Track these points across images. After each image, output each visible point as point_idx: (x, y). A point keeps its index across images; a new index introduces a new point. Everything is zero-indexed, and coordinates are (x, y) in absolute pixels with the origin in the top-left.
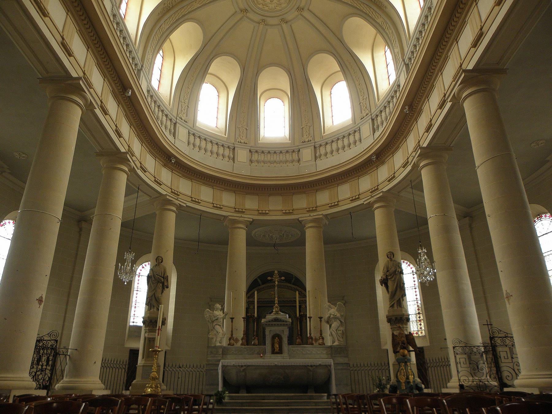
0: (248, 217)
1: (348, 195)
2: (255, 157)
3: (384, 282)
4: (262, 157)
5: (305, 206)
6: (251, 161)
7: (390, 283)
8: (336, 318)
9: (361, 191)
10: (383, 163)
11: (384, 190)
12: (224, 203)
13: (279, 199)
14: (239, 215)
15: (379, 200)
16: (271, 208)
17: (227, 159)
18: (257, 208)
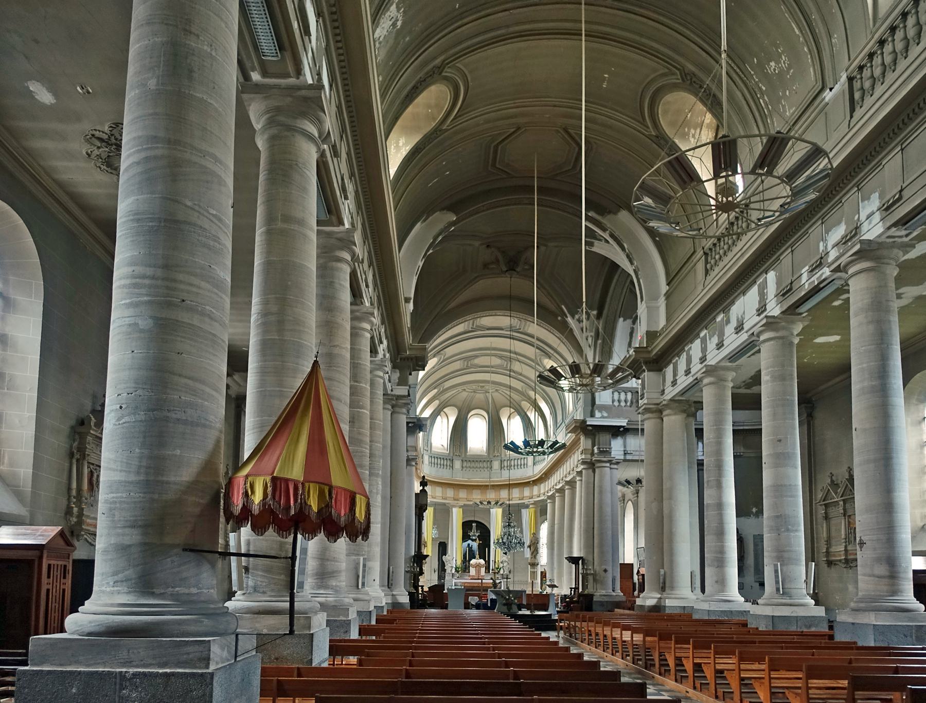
0: (461, 503)
1: (518, 496)
2: (465, 464)
3: (529, 547)
4: (469, 464)
5: (494, 497)
6: (462, 467)
7: (532, 548)
8: (505, 561)
9: (525, 495)
10: (536, 485)
11: (535, 500)
12: (448, 495)
13: (479, 491)
14: (456, 502)
15: (532, 504)
16: (474, 497)
17: (448, 467)
18: (466, 497)
